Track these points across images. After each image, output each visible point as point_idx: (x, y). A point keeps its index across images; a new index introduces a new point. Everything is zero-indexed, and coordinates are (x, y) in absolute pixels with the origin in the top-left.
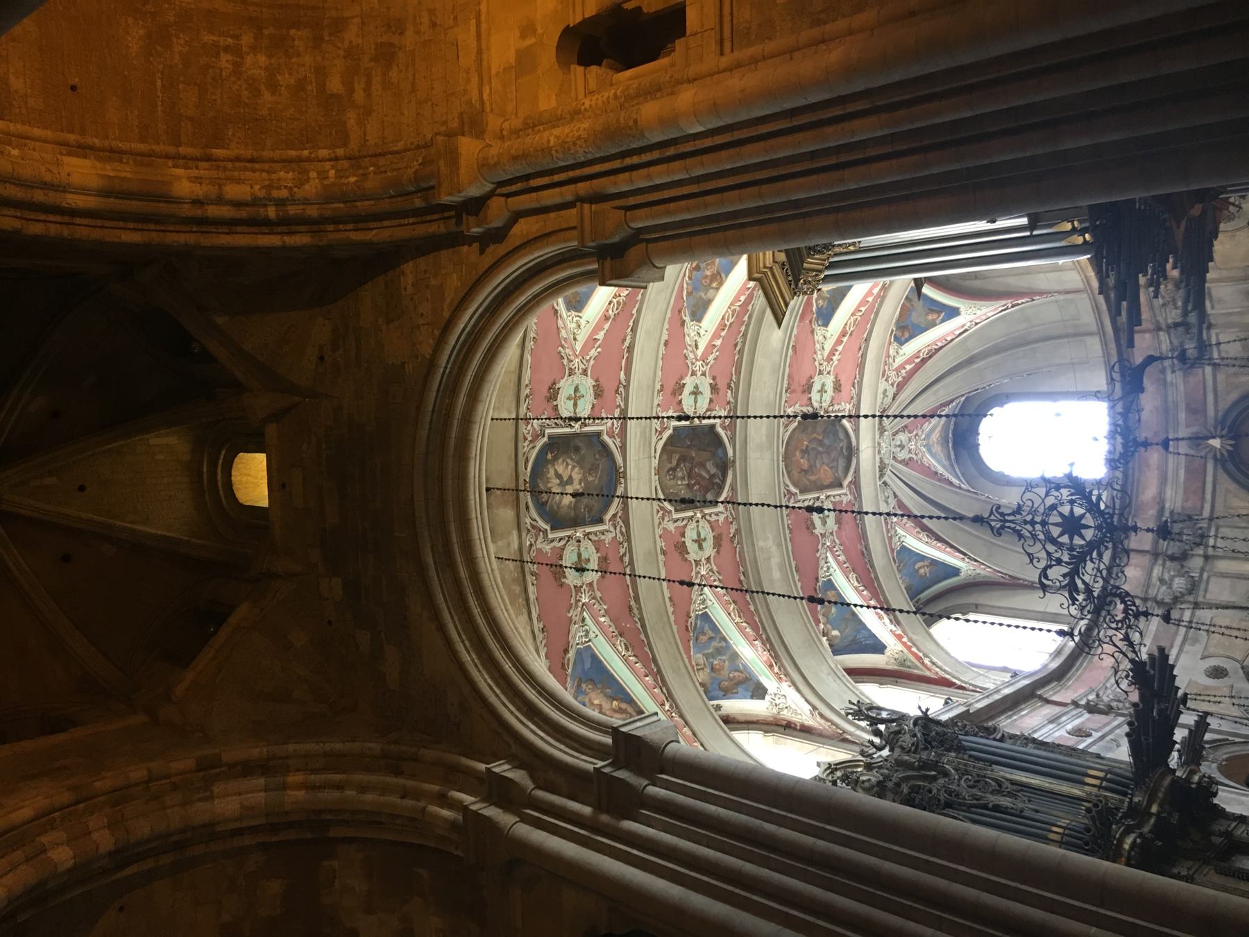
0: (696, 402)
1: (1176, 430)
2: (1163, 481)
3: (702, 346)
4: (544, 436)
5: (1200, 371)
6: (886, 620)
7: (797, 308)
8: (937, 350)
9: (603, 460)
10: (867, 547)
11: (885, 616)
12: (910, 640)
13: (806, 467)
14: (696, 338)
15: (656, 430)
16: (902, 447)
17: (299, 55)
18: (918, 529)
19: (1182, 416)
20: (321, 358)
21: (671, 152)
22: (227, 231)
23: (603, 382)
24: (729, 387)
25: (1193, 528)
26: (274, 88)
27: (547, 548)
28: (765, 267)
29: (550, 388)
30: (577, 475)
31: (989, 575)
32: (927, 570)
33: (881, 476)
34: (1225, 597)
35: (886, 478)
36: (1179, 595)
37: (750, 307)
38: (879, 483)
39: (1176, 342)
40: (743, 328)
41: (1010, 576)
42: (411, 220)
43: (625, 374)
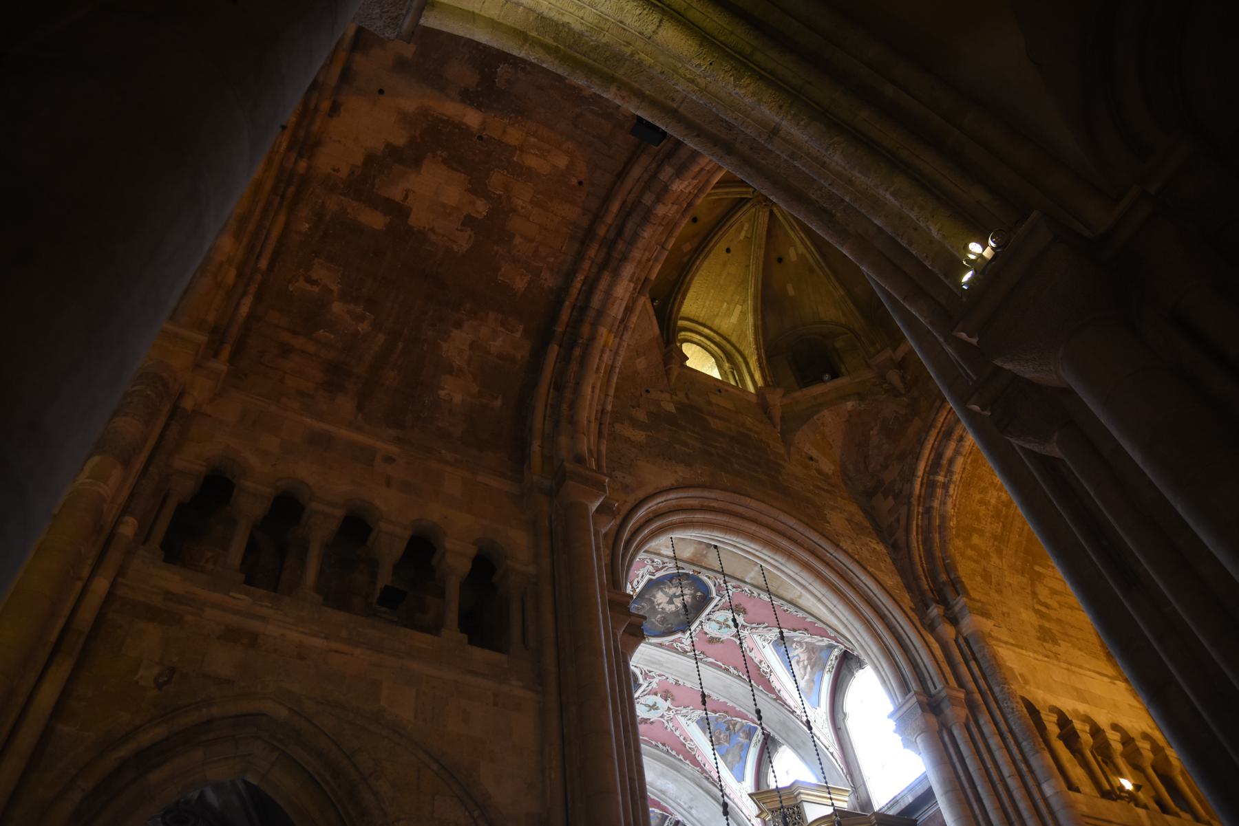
0: (645, 705)
3: (682, 720)
4: (717, 595)
7: (663, 796)
9: (663, 629)
14: (688, 717)
15: (650, 672)
17: (991, 523)
20: (811, 459)
21: (1023, 767)
22: (935, 446)
23: (719, 645)
26: (982, 502)
27: (641, 573)
28: (800, 793)
29: (744, 609)
30: (672, 608)
37: (688, 762)
40: (674, 753)
42: (925, 565)
43: (711, 663)
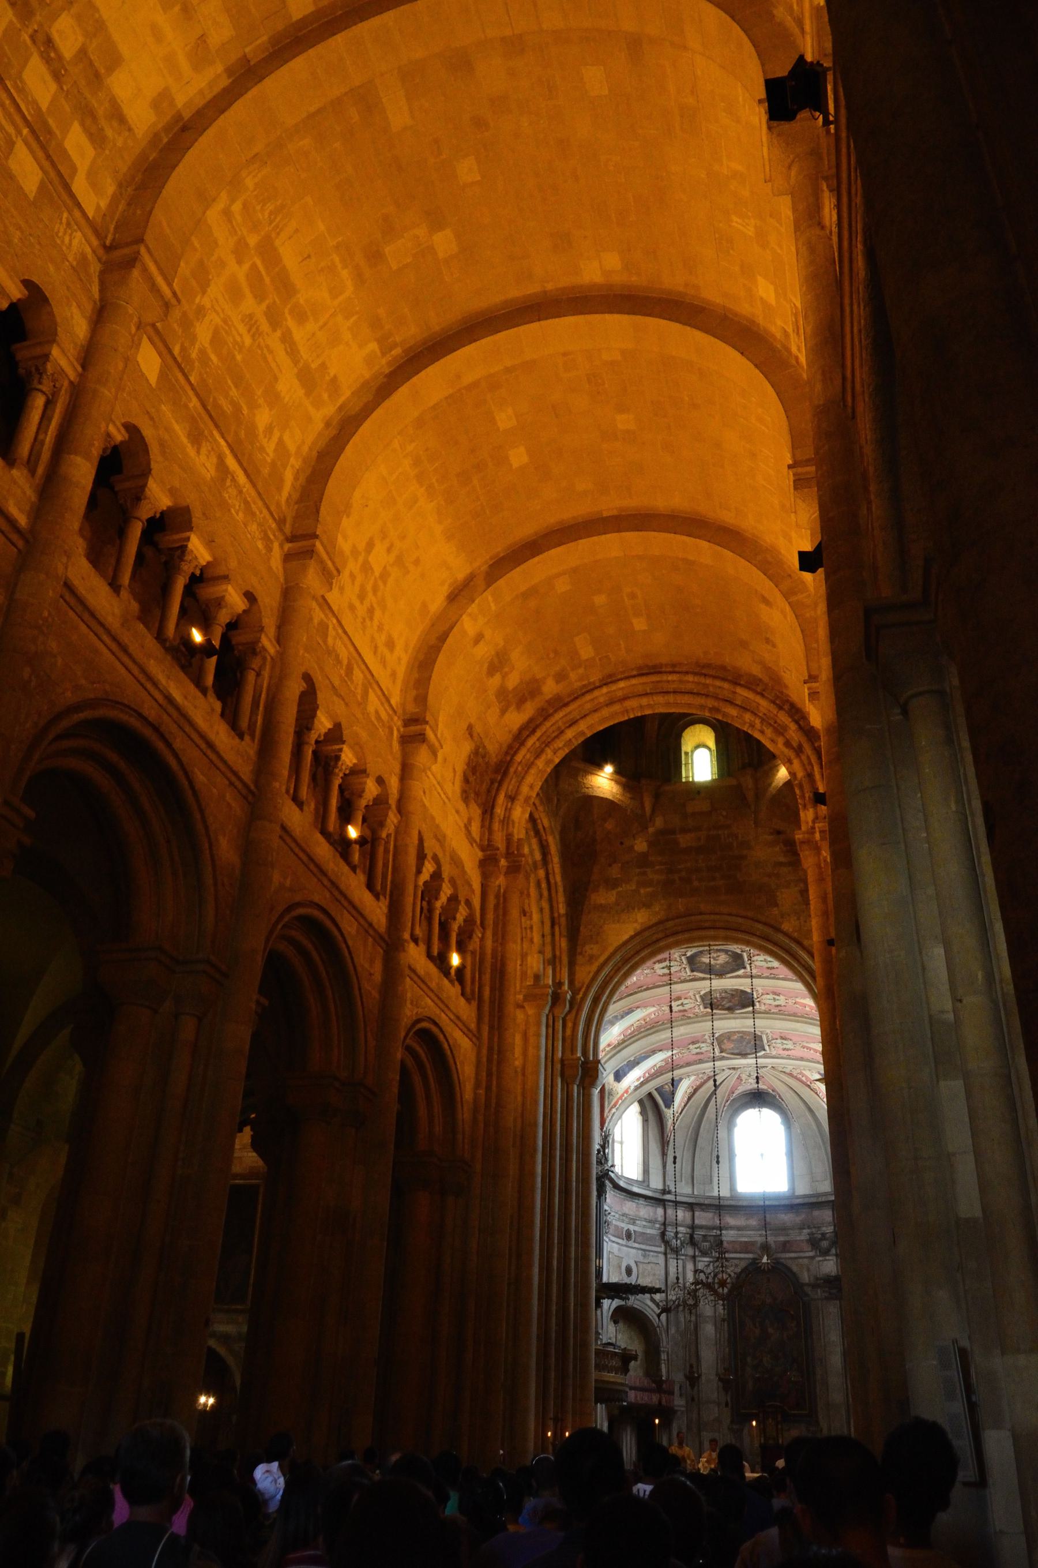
1: (771, 1235)
2: (739, 1228)
5: (810, 1249)
6: (637, 1083)
8: (816, 1093)
10: (682, 1067)
11: (640, 1082)
12: (626, 1098)
13: (732, 1038)
16: (750, 1076)
18: (695, 1087)
19: (782, 1239)
24: (780, 1011)
25: (711, 1248)
31: (668, 1130)
32: (668, 1090)
33: (730, 1069)
34: (672, 1270)
35: (728, 1070)
36: (670, 1243)
38: (724, 1068)
39: (828, 1235)
41: (669, 1141)
